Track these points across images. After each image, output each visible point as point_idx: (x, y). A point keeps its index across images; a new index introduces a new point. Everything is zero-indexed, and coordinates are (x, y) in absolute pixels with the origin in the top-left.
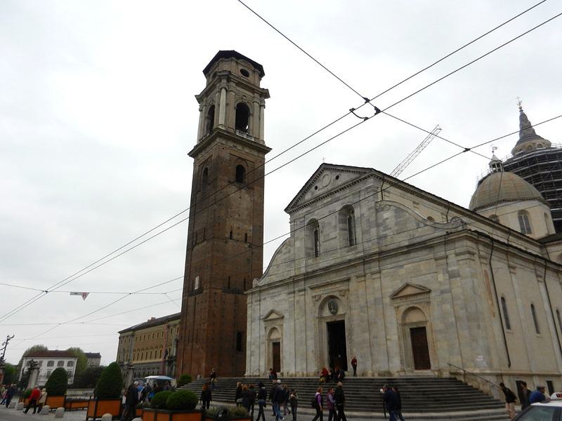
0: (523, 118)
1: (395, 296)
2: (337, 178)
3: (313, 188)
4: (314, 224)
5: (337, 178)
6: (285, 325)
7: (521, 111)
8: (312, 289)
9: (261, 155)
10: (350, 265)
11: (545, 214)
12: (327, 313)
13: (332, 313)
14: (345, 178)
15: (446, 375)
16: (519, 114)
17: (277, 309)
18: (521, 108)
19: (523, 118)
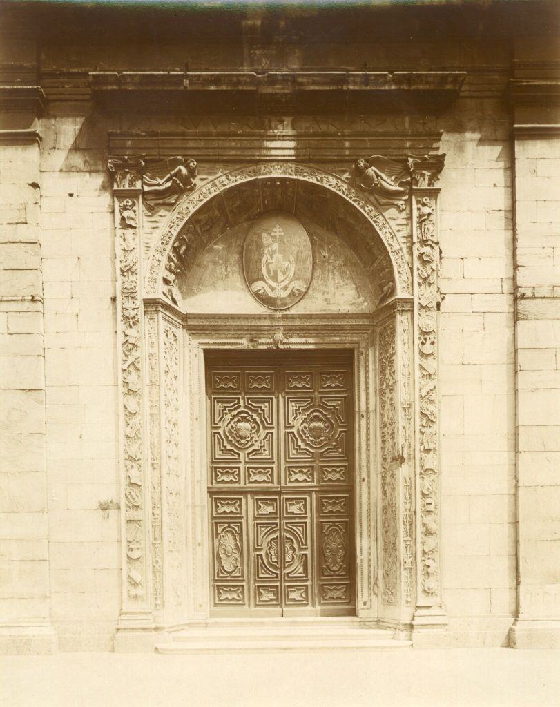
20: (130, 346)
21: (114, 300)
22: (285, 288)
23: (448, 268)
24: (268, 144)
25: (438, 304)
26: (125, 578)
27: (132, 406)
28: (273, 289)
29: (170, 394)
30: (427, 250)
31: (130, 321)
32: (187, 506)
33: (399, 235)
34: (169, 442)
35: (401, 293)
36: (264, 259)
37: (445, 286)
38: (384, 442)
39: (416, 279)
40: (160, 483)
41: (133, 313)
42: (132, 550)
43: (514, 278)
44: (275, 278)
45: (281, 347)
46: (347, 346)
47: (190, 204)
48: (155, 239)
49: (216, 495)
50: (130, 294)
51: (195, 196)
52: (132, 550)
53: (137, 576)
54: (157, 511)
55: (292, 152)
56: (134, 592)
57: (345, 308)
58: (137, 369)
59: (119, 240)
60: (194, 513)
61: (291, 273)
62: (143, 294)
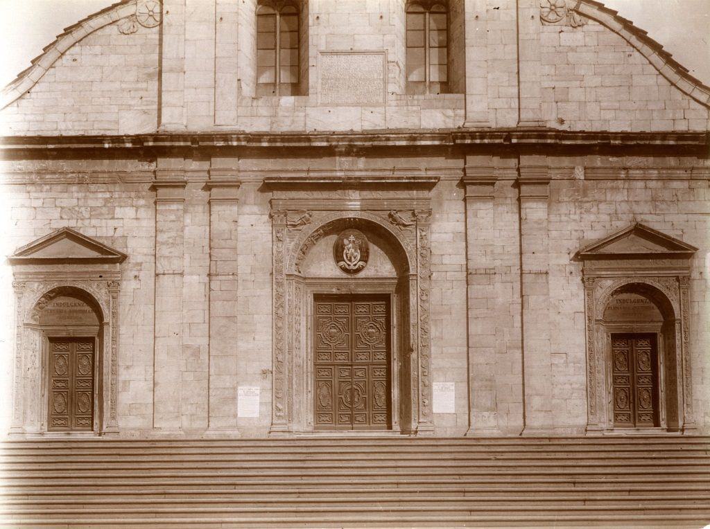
6: (129, 286)
12: (325, 268)
20: (279, 296)
21: (272, 274)
22: (355, 265)
23: (435, 260)
24: (347, 203)
25: (430, 277)
26: (274, 406)
27: (280, 324)
28: (349, 265)
29: (297, 318)
30: (424, 252)
31: (279, 284)
32: (303, 373)
33: (411, 244)
34: (296, 340)
35: (412, 272)
36: (345, 251)
37: (433, 268)
38: (404, 341)
39: (419, 264)
40: (292, 361)
41: (281, 281)
42: (278, 393)
43: (467, 264)
44: (350, 260)
45: (353, 293)
46: (387, 292)
47: (309, 229)
48: (291, 246)
49: (318, 367)
50: (280, 272)
51: (312, 225)
52: (278, 393)
53: (280, 407)
54: (290, 375)
55: (359, 207)
56: (278, 414)
57: (386, 274)
58: (282, 307)
59: (275, 247)
60: (307, 376)
61: (359, 257)
62: (286, 271)
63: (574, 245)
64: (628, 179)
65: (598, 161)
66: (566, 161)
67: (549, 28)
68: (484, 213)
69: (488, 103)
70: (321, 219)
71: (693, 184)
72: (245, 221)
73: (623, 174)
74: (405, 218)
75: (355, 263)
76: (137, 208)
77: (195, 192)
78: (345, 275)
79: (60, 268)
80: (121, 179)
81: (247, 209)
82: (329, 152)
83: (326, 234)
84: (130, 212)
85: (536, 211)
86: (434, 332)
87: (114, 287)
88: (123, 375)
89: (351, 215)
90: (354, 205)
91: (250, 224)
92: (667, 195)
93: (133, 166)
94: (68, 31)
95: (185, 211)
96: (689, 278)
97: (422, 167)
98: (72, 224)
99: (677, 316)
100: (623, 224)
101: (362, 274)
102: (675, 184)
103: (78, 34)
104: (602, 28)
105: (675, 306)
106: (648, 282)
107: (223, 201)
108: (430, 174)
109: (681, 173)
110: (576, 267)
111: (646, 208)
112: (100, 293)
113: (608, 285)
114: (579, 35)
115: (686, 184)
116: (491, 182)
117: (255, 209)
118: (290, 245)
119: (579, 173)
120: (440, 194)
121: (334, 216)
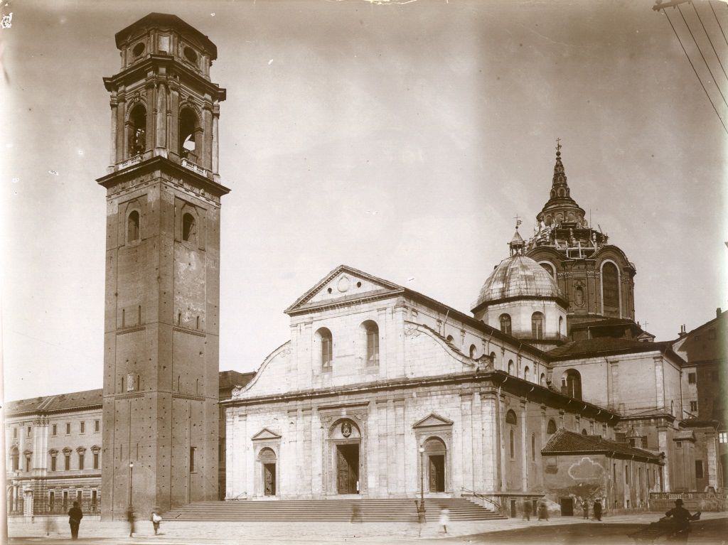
0: (559, 167)
1: (417, 426)
2: (359, 285)
3: (325, 289)
4: (325, 334)
5: (359, 285)
7: (558, 159)
8: (320, 409)
9: (216, 199)
10: (373, 388)
11: (561, 318)
12: (339, 436)
13: (344, 436)
14: (368, 287)
15: (458, 496)
16: (555, 162)
17: (270, 429)
18: (558, 154)
19: (559, 167)
50: (323, 438)
63: (412, 422)
64: (431, 396)
65: (421, 389)
66: (410, 391)
67: (409, 337)
68: (383, 411)
69: (390, 370)
70: (335, 419)
71: (454, 396)
72: (313, 421)
73: (429, 394)
74: (359, 417)
75: (347, 434)
76: (284, 419)
77: (300, 412)
78: (344, 438)
79: (263, 441)
80: (279, 410)
81: (314, 417)
82: (336, 395)
83: (338, 424)
84: (282, 420)
85: (400, 411)
86: (368, 458)
87: (278, 446)
88: (282, 476)
89: (343, 417)
90: (344, 413)
91: (315, 420)
92: (444, 401)
93: (283, 405)
94: (267, 358)
95: (297, 419)
96: (451, 433)
97: (364, 398)
98: (265, 426)
99: (448, 448)
100: (429, 414)
101: (350, 437)
102: (447, 396)
103: (269, 359)
104: (426, 335)
105: (447, 444)
106: (437, 436)
107: (306, 415)
108: (368, 400)
109: (449, 392)
110: (413, 431)
111: (437, 406)
112: (275, 450)
113: (424, 438)
114: (418, 339)
115: (451, 396)
116: (386, 401)
117: (316, 417)
118: (326, 431)
119: (414, 395)
120: (370, 409)
121: (339, 418)
